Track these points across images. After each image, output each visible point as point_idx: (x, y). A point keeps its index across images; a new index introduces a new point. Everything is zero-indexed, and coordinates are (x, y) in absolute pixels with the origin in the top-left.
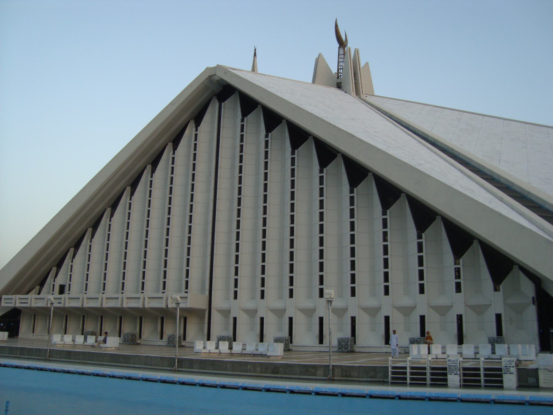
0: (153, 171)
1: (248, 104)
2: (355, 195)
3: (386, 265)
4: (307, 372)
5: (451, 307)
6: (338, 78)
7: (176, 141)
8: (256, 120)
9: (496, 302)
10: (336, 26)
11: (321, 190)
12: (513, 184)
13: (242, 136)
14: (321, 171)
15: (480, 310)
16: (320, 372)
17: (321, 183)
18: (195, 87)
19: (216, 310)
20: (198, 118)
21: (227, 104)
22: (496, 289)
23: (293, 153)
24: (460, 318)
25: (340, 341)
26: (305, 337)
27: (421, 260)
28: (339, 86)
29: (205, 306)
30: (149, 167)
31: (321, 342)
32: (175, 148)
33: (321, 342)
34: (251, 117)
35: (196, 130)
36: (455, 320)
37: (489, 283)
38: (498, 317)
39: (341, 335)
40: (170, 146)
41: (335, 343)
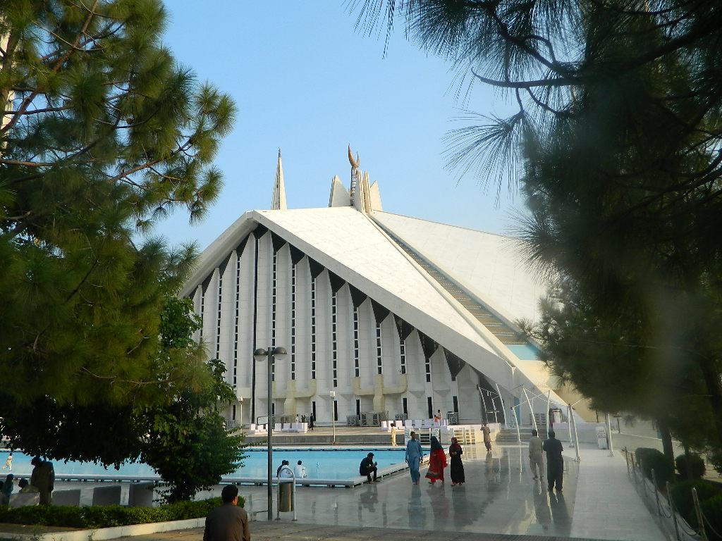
0: (204, 291)
1: (278, 242)
2: (357, 312)
3: (380, 363)
4: (321, 440)
5: (423, 393)
6: (351, 195)
7: (222, 267)
8: (284, 255)
9: (454, 389)
10: (349, 151)
11: (334, 308)
12: (477, 298)
13: (275, 266)
14: (334, 295)
15: (443, 394)
16: (329, 440)
17: (334, 303)
18: (237, 227)
19: (260, 399)
20: (240, 249)
21: (262, 240)
22: (454, 379)
23: (313, 281)
24: (430, 399)
25: (348, 418)
26: (323, 416)
27: (403, 359)
28: (352, 205)
29: (251, 397)
30: (200, 287)
31: (336, 419)
32: (222, 273)
33: (336, 419)
34: (280, 251)
35: (239, 260)
36: (427, 401)
37: (449, 375)
38: (455, 398)
39: (349, 414)
40: (217, 272)
41: (345, 420)
